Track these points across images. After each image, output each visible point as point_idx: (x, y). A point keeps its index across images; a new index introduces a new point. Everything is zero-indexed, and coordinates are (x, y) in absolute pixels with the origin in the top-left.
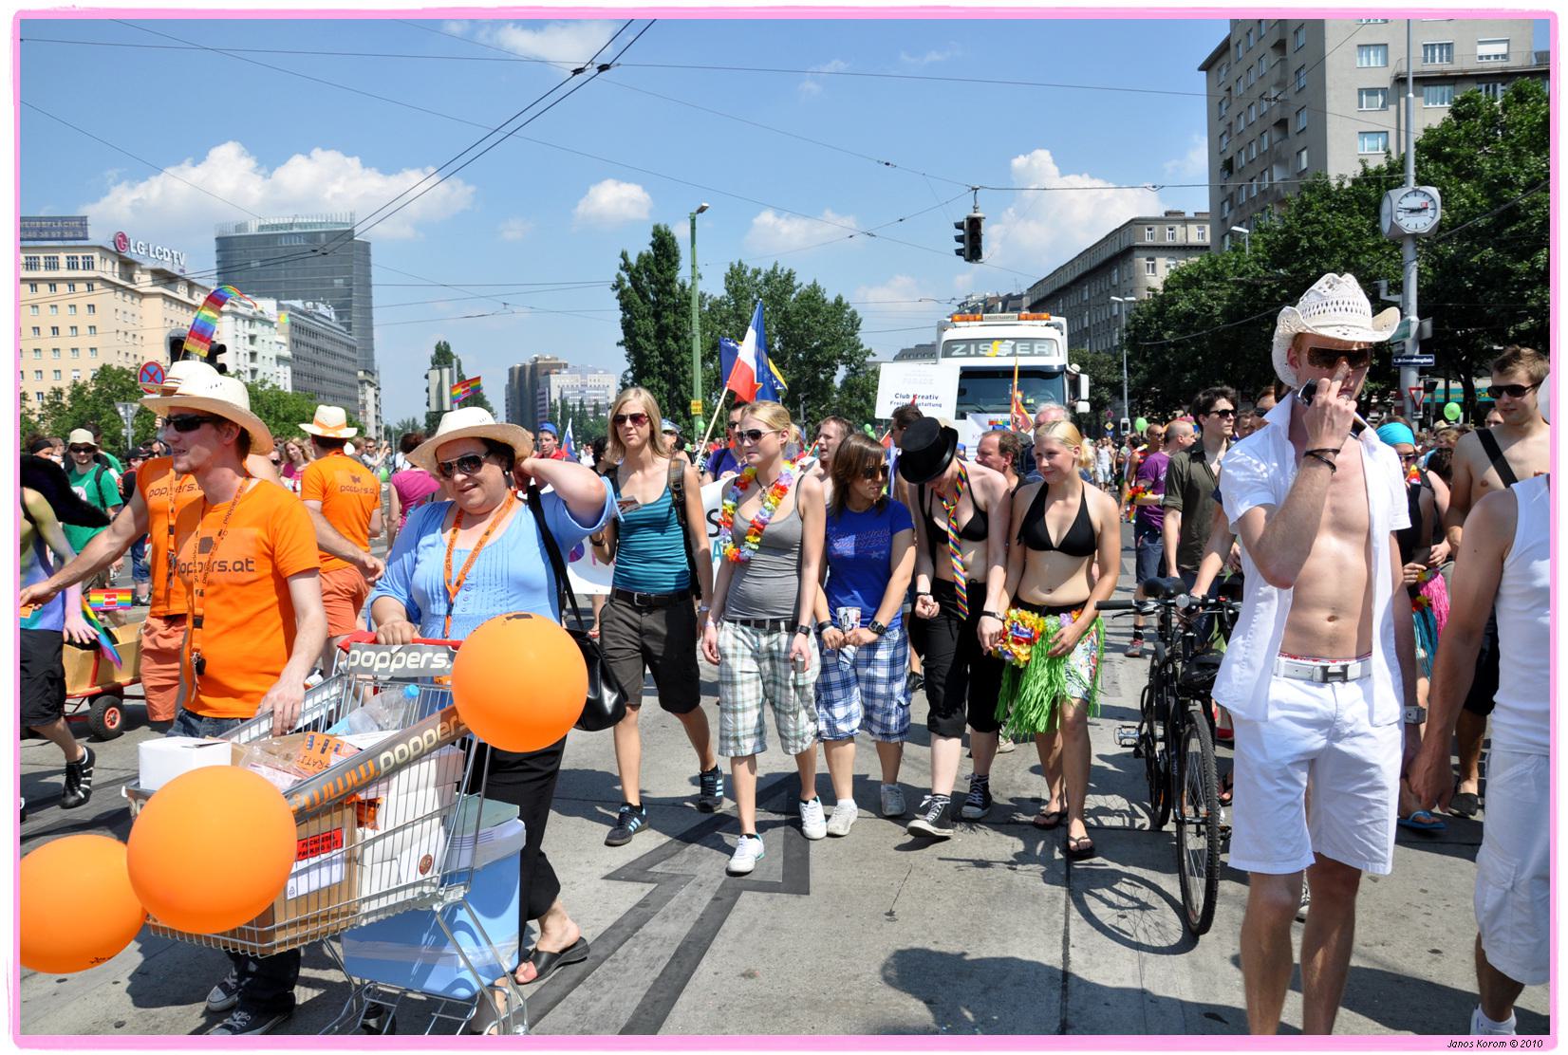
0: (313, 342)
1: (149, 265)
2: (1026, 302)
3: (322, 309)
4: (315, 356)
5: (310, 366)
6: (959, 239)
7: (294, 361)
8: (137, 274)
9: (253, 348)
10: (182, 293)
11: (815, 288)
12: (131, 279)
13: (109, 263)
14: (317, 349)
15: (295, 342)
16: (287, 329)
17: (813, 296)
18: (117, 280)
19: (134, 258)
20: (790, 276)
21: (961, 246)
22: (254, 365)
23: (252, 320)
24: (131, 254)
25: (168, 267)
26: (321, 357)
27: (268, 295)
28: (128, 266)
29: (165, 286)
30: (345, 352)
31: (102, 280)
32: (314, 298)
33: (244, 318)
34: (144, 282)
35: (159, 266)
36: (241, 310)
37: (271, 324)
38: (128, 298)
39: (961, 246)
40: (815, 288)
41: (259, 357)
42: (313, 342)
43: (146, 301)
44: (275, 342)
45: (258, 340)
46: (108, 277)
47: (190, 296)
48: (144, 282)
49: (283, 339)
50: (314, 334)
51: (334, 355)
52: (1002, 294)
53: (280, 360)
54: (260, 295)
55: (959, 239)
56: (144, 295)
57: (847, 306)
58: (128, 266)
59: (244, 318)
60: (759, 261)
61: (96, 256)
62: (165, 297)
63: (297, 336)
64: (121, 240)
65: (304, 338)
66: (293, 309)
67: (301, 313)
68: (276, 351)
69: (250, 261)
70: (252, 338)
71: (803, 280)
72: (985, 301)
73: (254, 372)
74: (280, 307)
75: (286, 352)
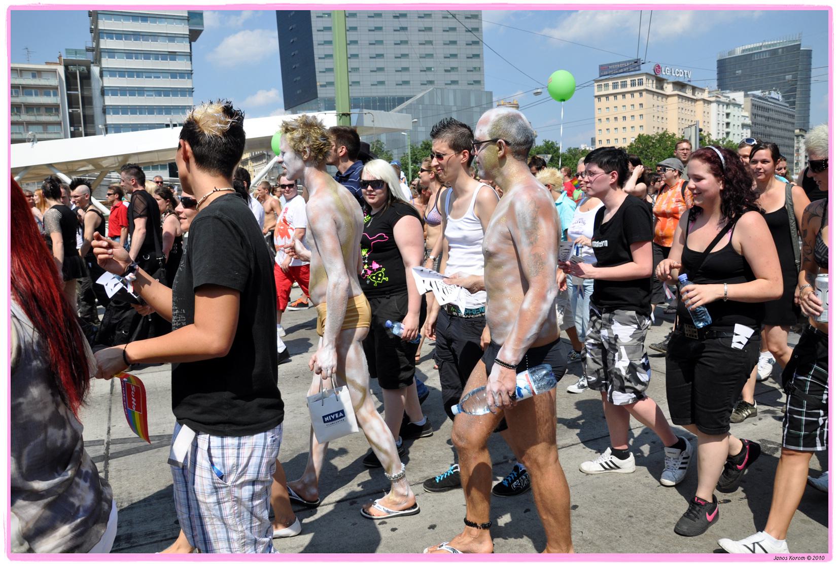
0: (766, 114)
1: (672, 80)
3: (774, 94)
4: (767, 123)
5: (763, 128)
7: (752, 127)
8: (665, 85)
9: (728, 120)
10: (689, 93)
12: (662, 88)
13: (651, 81)
14: (768, 118)
15: (754, 115)
19: (664, 77)
22: (728, 130)
23: (728, 105)
24: (662, 75)
25: (681, 80)
26: (770, 123)
27: (740, 90)
28: (660, 82)
29: (680, 90)
30: (787, 119)
32: (768, 88)
33: (723, 103)
34: (669, 89)
35: (677, 80)
36: (723, 99)
37: (739, 106)
38: (660, 98)
41: (731, 125)
42: (766, 114)
43: (669, 99)
44: (742, 115)
45: (731, 115)
46: (650, 89)
47: (693, 94)
48: (669, 89)
49: (747, 114)
50: (767, 110)
51: (779, 121)
53: (744, 126)
54: (736, 89)
56: (668, 96)
59: (723, 103)
61: (644, 78)
62: (679, 95)
63: (755, 111)
64: (658, 68)
65: (760, 112)
66: (754, 96)
67: (760, 98)
68: (742, 121)
69: (731, 73)
70: (728, 115)
73: (728, 134)
74: (746, 96)
75: (748, 121)
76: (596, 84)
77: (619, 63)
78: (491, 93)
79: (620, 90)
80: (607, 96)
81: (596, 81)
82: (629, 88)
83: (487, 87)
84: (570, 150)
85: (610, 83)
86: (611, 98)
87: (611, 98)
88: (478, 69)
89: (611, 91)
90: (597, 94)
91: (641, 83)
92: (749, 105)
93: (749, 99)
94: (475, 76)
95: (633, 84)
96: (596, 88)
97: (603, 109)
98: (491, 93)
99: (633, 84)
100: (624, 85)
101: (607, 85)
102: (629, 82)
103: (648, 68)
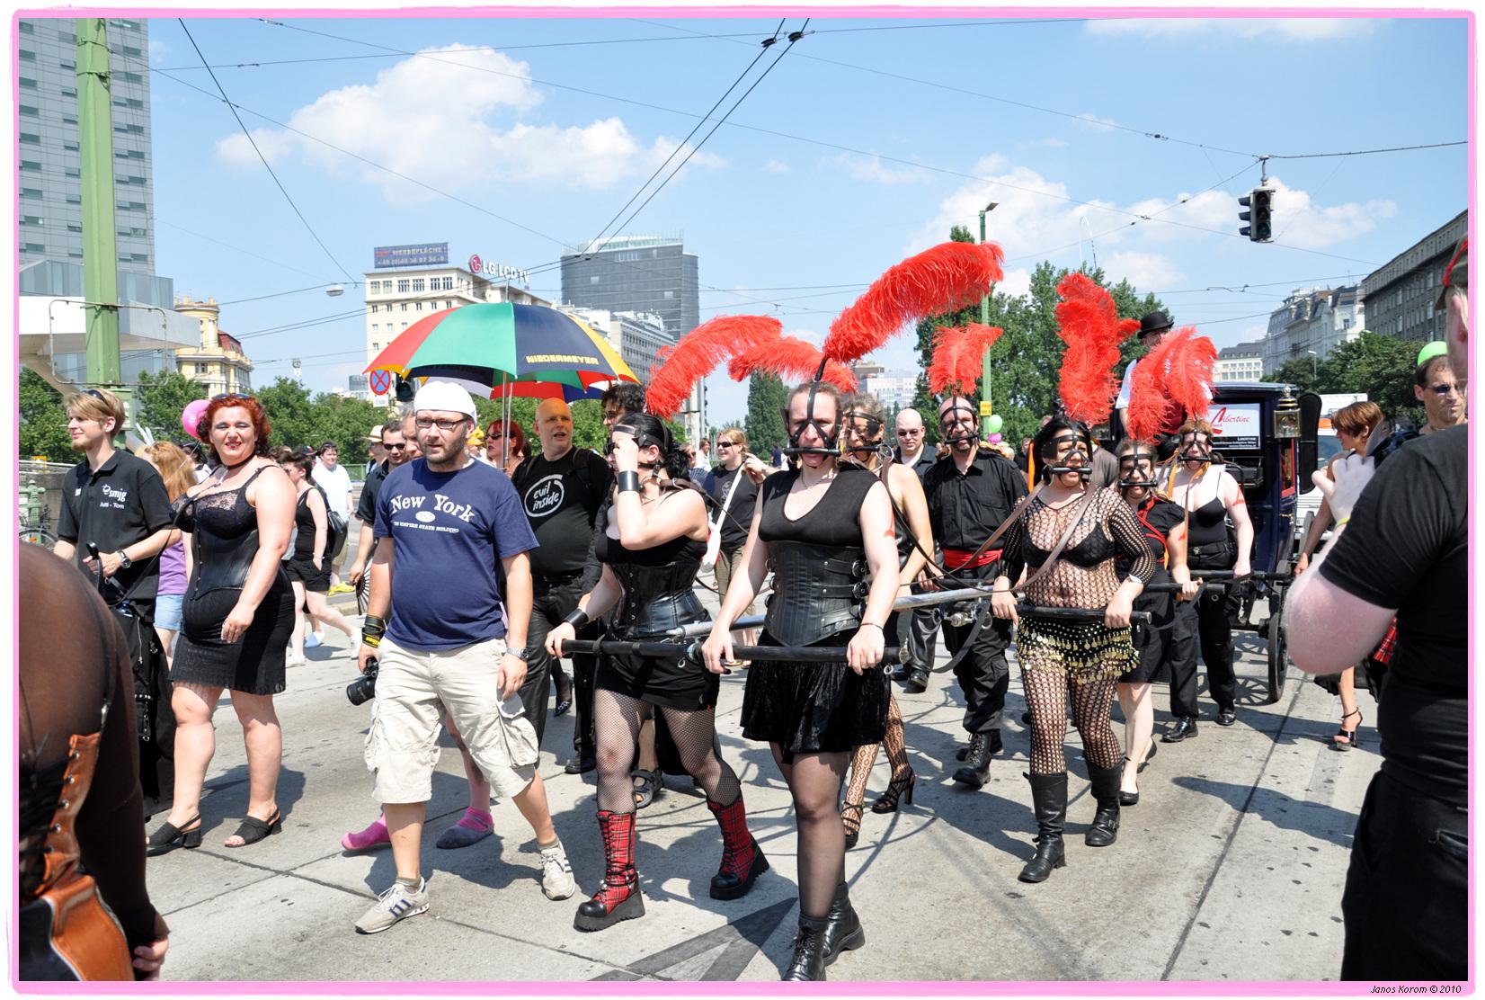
0: (643, 350)
2: (1360, 294)
6: (1244, 217)
8: (488, 292)
11: (1124, 287)
12: (483, 297)
14: (647, 356)
16: (619, 337)
17: (1123, 292)
18: (471, 298)
20: (1098, 276)
21: (1246, 224)
24: (482, 274)
25: (514, 285)
28: (480, 285)
31: (459, 298)
39: (1246, 224)
40: (1124, 287)
46: (464, 295)
52: (1334, 287)
54: (597, 307)
55: (1244, 217)
57: (1158, 305)
58: (480, 285)
60: (1066, 261)
61: (454, 276)
63: (628, 344)
64: (476, 262)
65: (634, 346)
66: (625, 320)
67: (633, 323)
71: (1112, 279)
72: (1313, 296)
74: (613, 318)
76: (368, 281)
77: (411, 247)
78: (170, 281)
79: (411, 294)
80: (389, 304)
81: (368, 275)
82: (428, 292)
83: (161, 270)
84: (321, 398)
85: (395, 280)
86: (397, 307)
87: (397, 307)
88: (142, 233)
89: (395, 294)
90: (371, 298)
91: (448, 286)
92: (619, 331)
93: (618, 323)
94: (136, 246)
95: (435, 286)
96: (368, 287)
97: (382, 325)
98: (170, 281)
99: (435, 286)
100: (419, 286)
101: (388, 284)
102: (427, 283)
103: (458, 258)
